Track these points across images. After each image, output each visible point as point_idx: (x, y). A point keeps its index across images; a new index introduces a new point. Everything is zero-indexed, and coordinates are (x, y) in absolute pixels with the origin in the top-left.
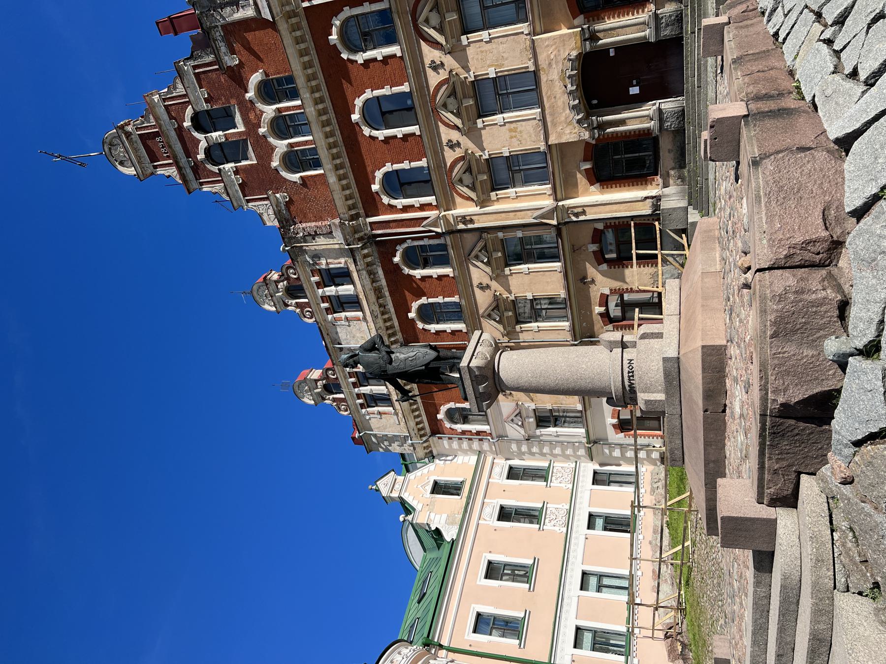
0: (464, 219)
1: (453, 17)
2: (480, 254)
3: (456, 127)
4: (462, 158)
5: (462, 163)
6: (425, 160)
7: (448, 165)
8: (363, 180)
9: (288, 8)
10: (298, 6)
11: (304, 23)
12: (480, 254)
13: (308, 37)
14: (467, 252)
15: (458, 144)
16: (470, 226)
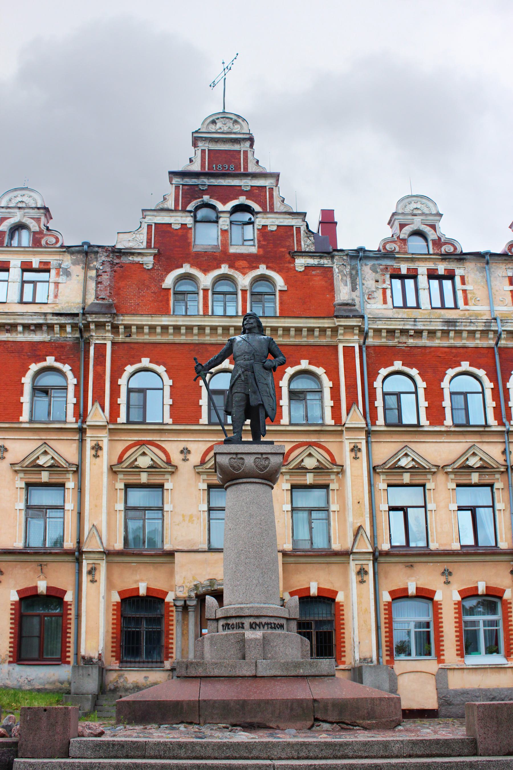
0: (97, 448)
1: (309, 479)
2: (49, 457)
3: (203, 462)
4: (169, 462)
5: (164, 458)
6: (170, 421)
7: (163, 445)
8: (159, 352)
9: (341, 331)
10: (341, 341)
11: (324, 341)
12: (49, 457)
13: (312, 341)
14: (51, 443)
15: (185, 460)
16: (89, 453)
